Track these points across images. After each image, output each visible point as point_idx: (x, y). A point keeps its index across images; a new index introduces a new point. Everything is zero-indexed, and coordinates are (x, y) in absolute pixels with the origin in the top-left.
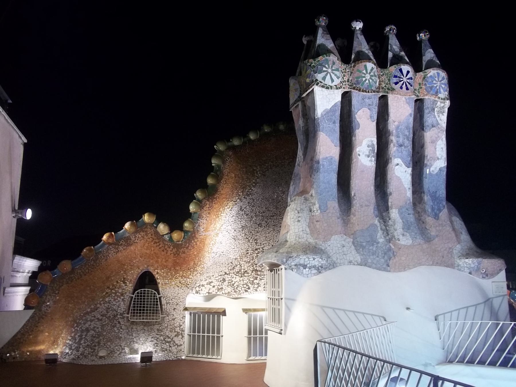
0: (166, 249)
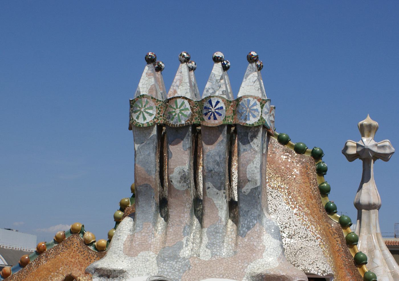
0: (90, 258)
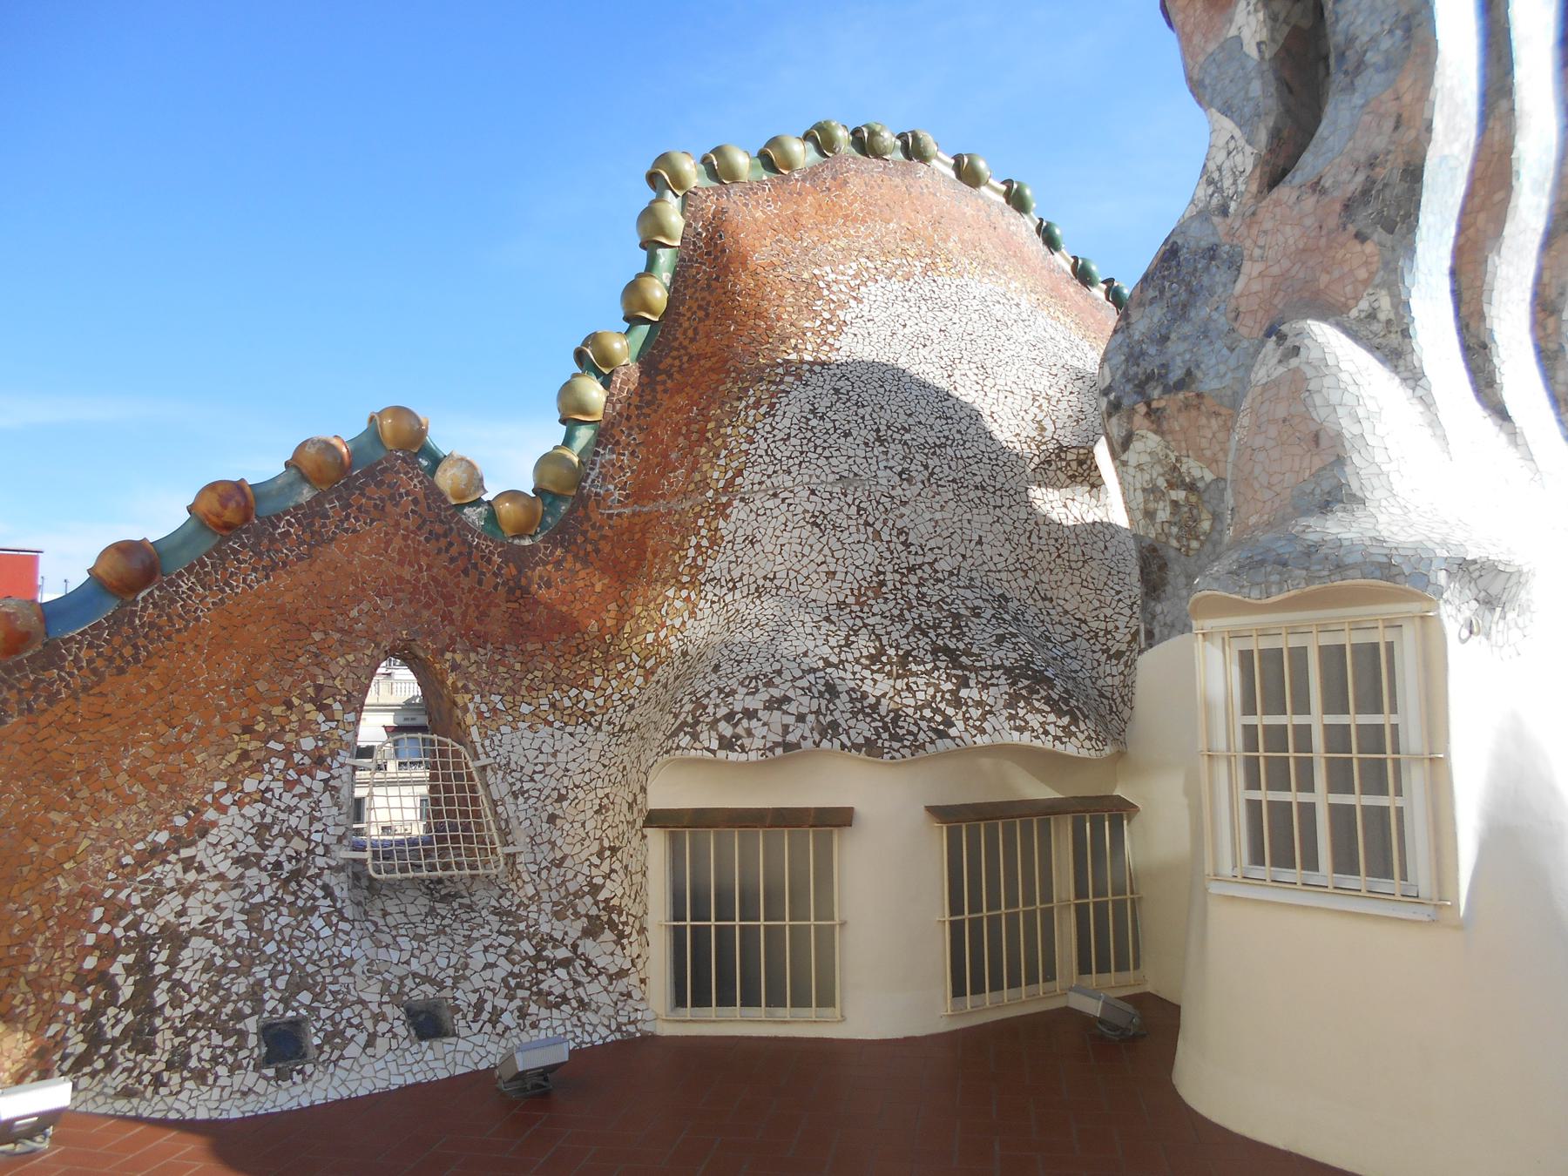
0: (475, 566)
